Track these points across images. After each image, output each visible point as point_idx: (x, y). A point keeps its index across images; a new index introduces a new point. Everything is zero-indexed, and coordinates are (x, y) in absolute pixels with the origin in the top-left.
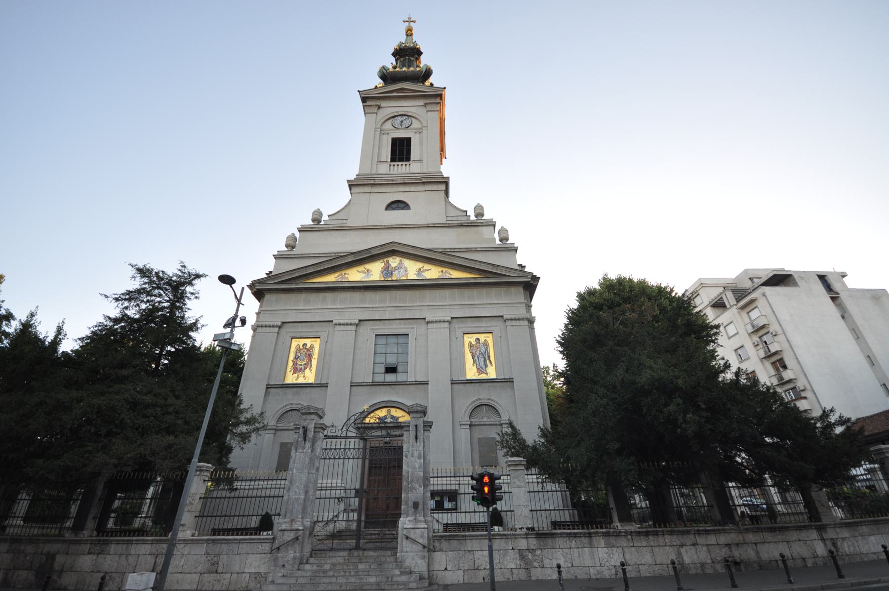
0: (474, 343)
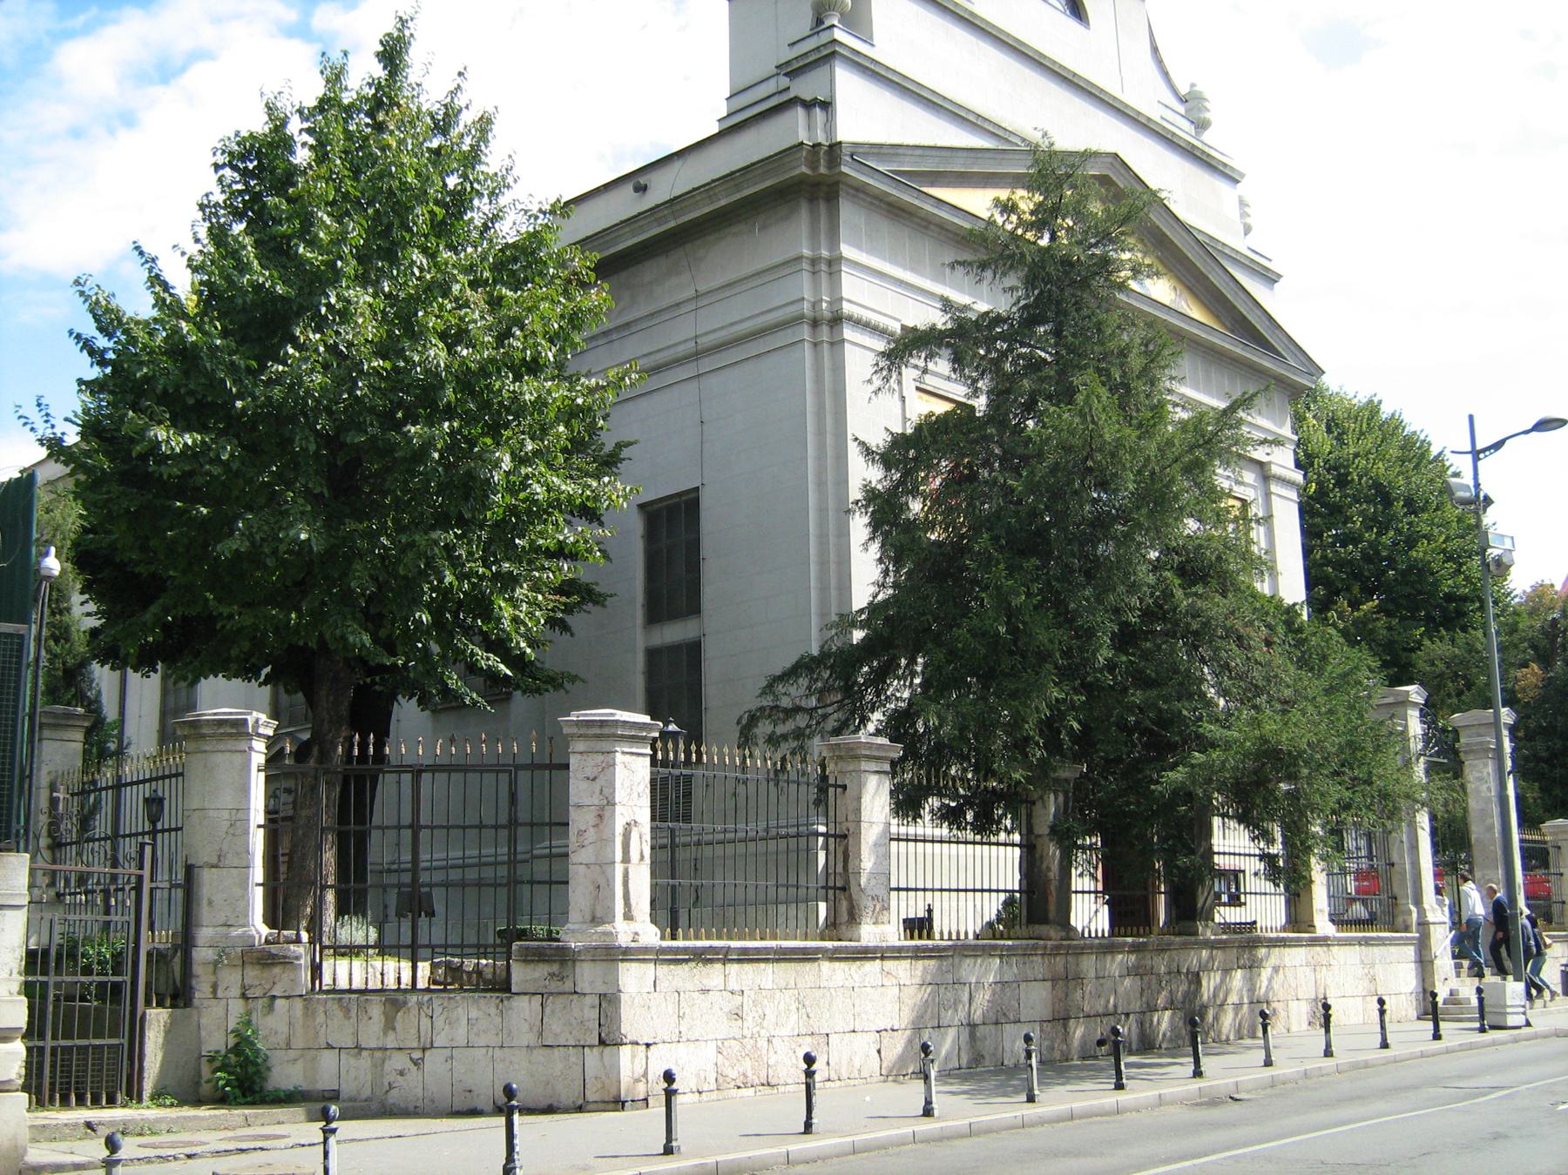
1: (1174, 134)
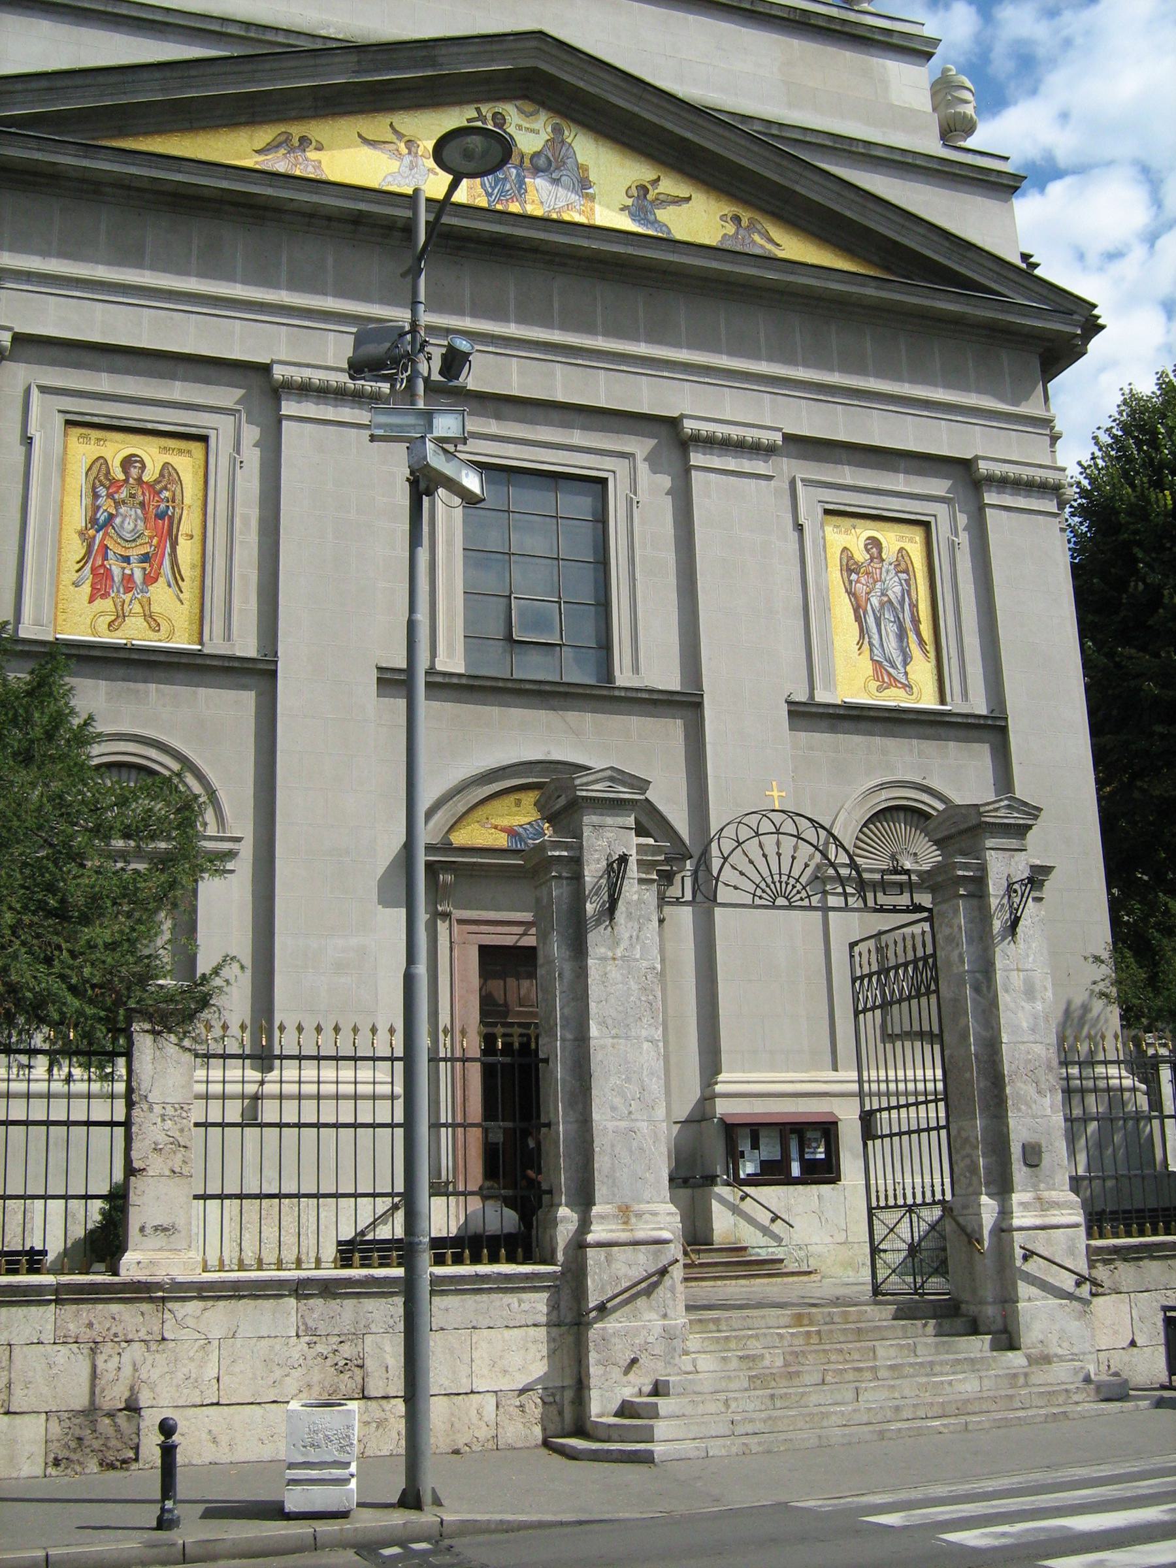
0: (861, 556)
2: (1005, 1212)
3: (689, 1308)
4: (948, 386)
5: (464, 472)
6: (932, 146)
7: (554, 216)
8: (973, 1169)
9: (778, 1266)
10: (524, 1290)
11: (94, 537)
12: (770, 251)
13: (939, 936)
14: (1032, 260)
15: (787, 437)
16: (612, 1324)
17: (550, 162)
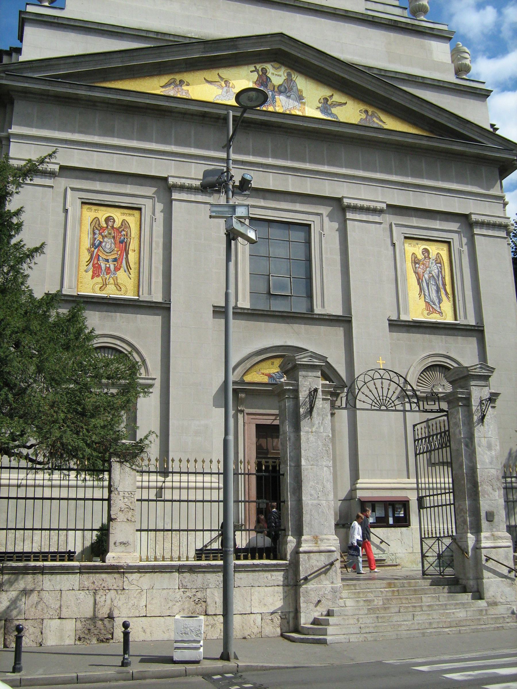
0: (420, 256)
1: (373, 17)
2: (478, 541)
3: (343, 579)
4: (458, 182)
5: (249, 230)
6: (451, 78)
7: (288, 112)
8: (465, 522)
9: (383, 562)
10: (273, 571)
11: (94, 251)
12: (381, 126)
13: (451, 423)
14: (495, 127)
15: (388, 206)
16: (310, 586)
17: (286, 89)
